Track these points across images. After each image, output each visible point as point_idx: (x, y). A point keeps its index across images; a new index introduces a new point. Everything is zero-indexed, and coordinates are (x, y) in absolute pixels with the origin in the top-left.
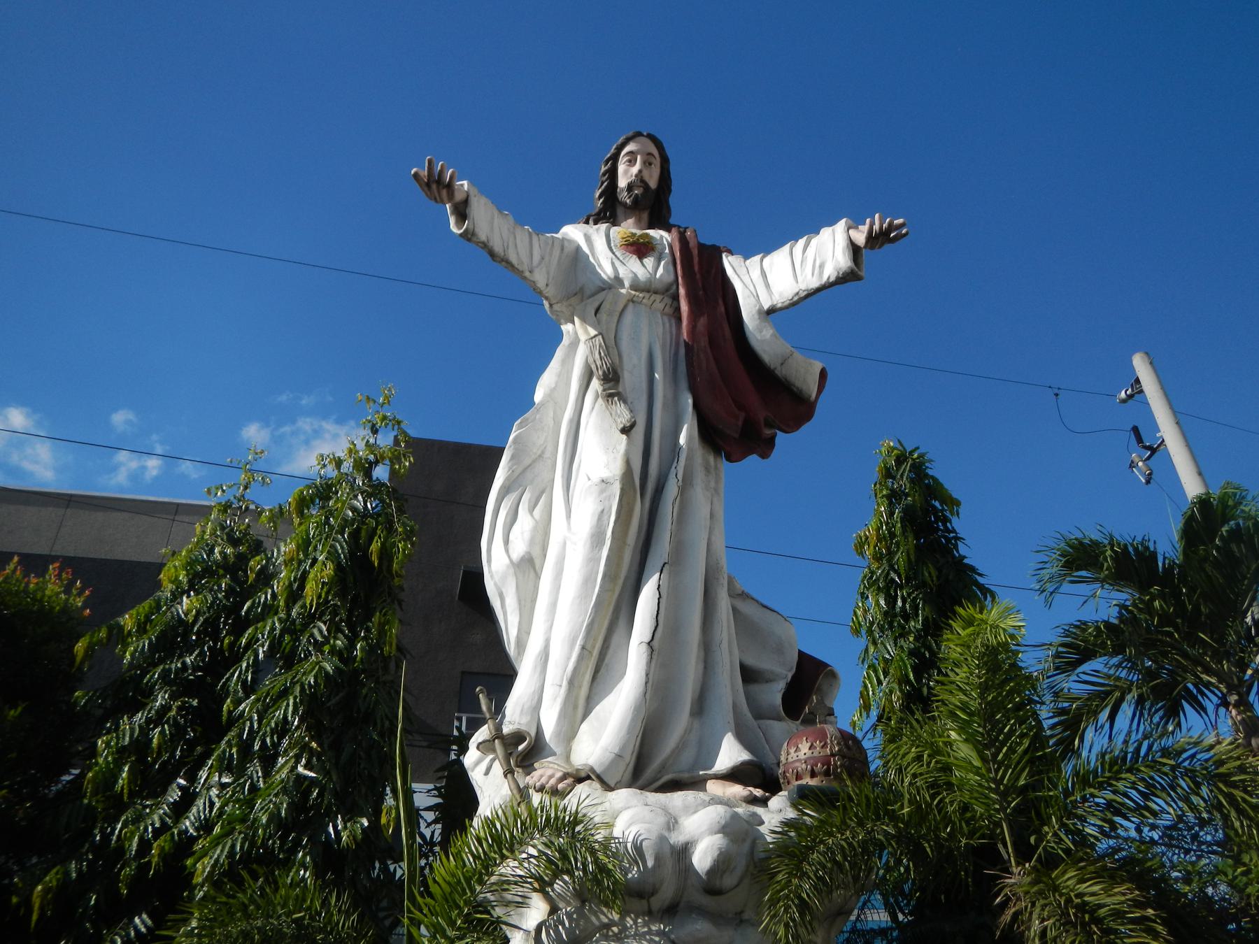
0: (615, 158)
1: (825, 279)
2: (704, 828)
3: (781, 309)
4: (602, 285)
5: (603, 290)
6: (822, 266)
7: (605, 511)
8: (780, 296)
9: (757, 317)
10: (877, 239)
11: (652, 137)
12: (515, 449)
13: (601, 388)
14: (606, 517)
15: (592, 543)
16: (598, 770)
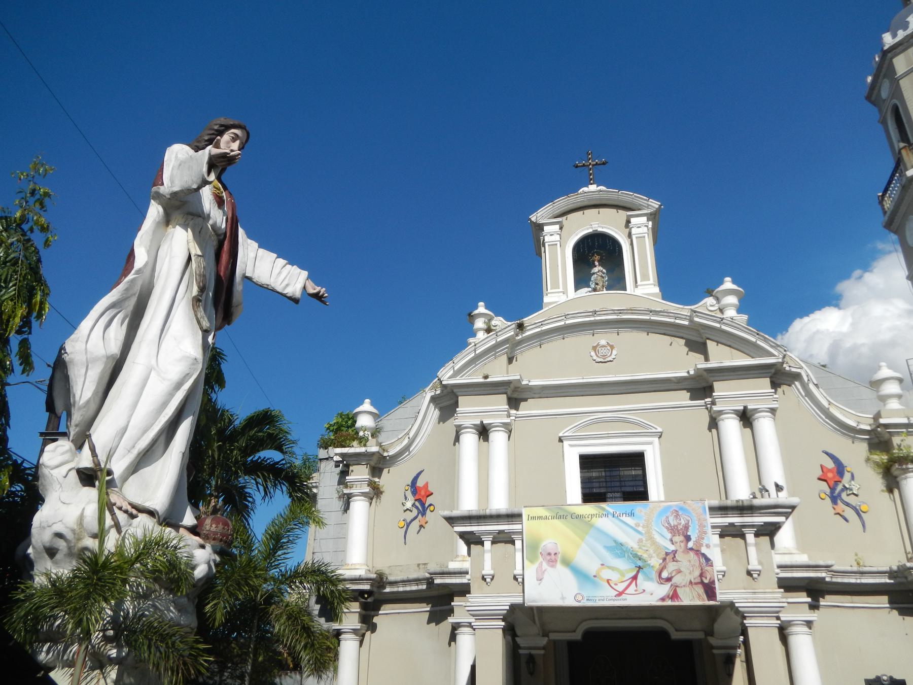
0: (227, 128)
1: (285, 292)
2: (203, 560)
3: (253, 282)
4: (201, 213)
5: (200, 216)
6: (287, 285)
7: (189, 375)
8: (258, 277)
9: (241, 276)
10: (317, 296)
11: (248, 134)
12: (130, 285)
13: (197, 293)
14: (187, 378)
15: (176, 386)
16: (160, 514)
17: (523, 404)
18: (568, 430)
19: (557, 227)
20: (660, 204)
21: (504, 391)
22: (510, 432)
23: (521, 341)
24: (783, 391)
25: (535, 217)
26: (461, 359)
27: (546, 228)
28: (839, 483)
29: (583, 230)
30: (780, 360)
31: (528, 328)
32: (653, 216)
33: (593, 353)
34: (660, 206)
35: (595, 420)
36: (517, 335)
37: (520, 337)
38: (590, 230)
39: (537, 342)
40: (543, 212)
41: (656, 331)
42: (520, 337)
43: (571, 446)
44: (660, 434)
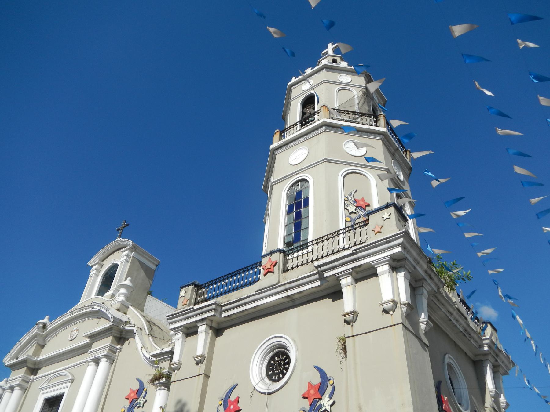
17: (40, 371)
18: (45, 382)
19: (96, 266)
20: (132, 241)
21: (25, 365)
22: (26, 389)
23: (48, 334)
24: (129, 342)
25: (90, 263)
26: (14, 351)
27: (94, 268)
28: (136, 400)
29: (109, 265)
30: (111, 324)
31: (48, 327)
32: (133, 250)
33: (70, 336)
34: (132, 242)
35: (54, 376)
36: (44, 332)
37: (45, 332)
38: (111, 264)
39: (54, 334)
40: (93, 260)
41: (97, 317)
42: (44, 333)
43: (43, 394)
44: (71, 380)
